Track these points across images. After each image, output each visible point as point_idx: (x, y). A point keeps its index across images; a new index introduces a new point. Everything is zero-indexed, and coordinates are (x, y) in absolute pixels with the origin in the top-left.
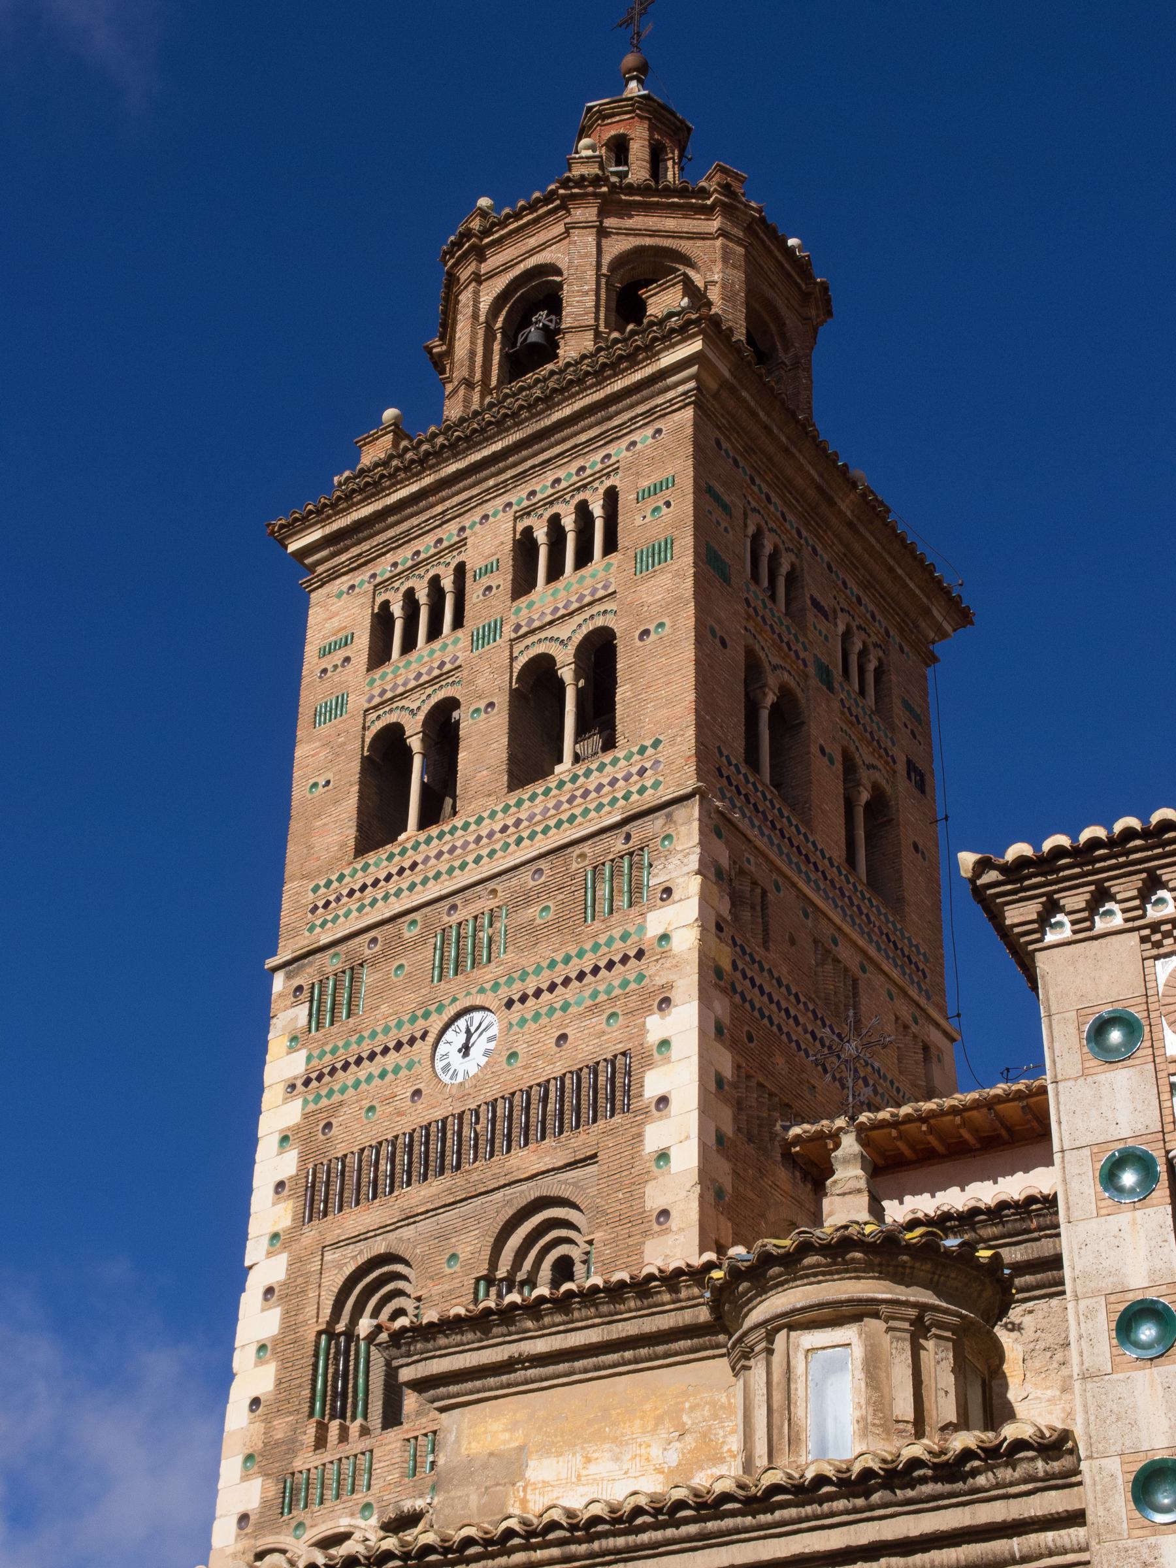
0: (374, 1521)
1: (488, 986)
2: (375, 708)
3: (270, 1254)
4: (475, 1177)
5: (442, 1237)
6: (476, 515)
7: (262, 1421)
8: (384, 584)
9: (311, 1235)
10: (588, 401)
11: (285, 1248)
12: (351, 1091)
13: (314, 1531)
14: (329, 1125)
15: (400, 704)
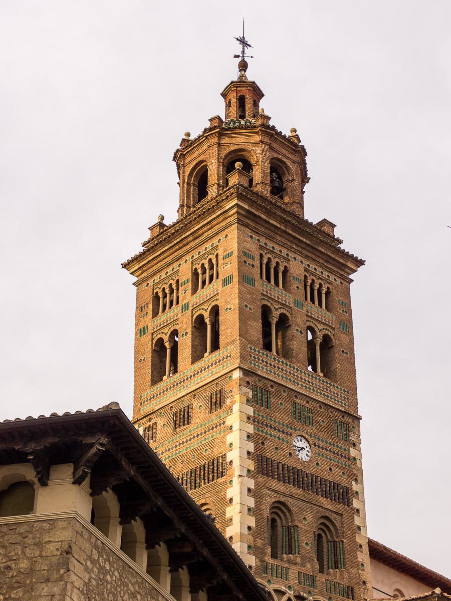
0: (292, 592)
1: (309, 434)
2: (264, 295)
3: (247, 476)
4: (310, 497)
5: (302, 510)
6: (292, 255)
7: (253, 536)
8: (261, 247)
9: (261, 479)
10: (328, 253)
11: (253, 477)
12: (269, 437)
13: (275, 585)
14: (263, 443)
15: (272, 302)
